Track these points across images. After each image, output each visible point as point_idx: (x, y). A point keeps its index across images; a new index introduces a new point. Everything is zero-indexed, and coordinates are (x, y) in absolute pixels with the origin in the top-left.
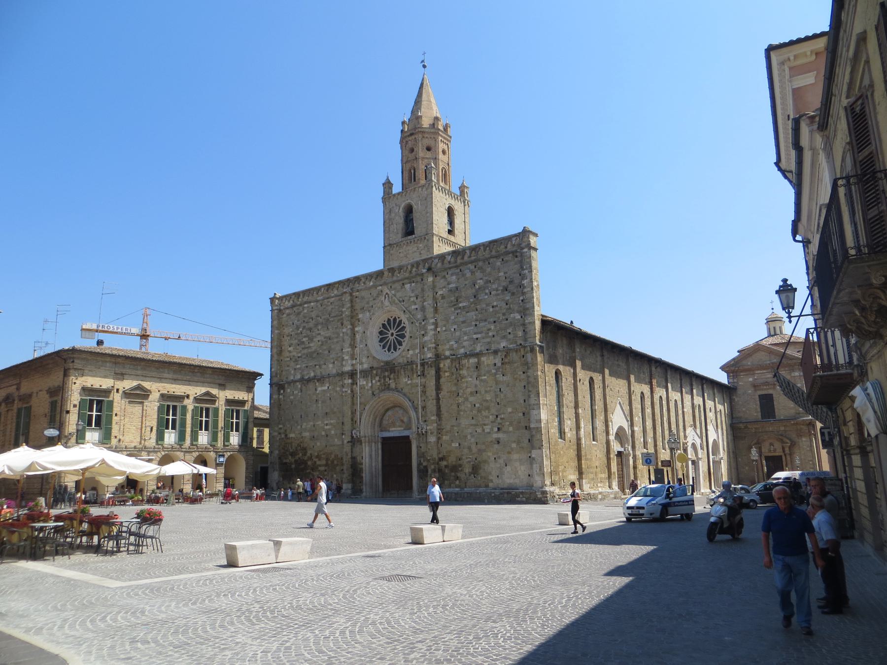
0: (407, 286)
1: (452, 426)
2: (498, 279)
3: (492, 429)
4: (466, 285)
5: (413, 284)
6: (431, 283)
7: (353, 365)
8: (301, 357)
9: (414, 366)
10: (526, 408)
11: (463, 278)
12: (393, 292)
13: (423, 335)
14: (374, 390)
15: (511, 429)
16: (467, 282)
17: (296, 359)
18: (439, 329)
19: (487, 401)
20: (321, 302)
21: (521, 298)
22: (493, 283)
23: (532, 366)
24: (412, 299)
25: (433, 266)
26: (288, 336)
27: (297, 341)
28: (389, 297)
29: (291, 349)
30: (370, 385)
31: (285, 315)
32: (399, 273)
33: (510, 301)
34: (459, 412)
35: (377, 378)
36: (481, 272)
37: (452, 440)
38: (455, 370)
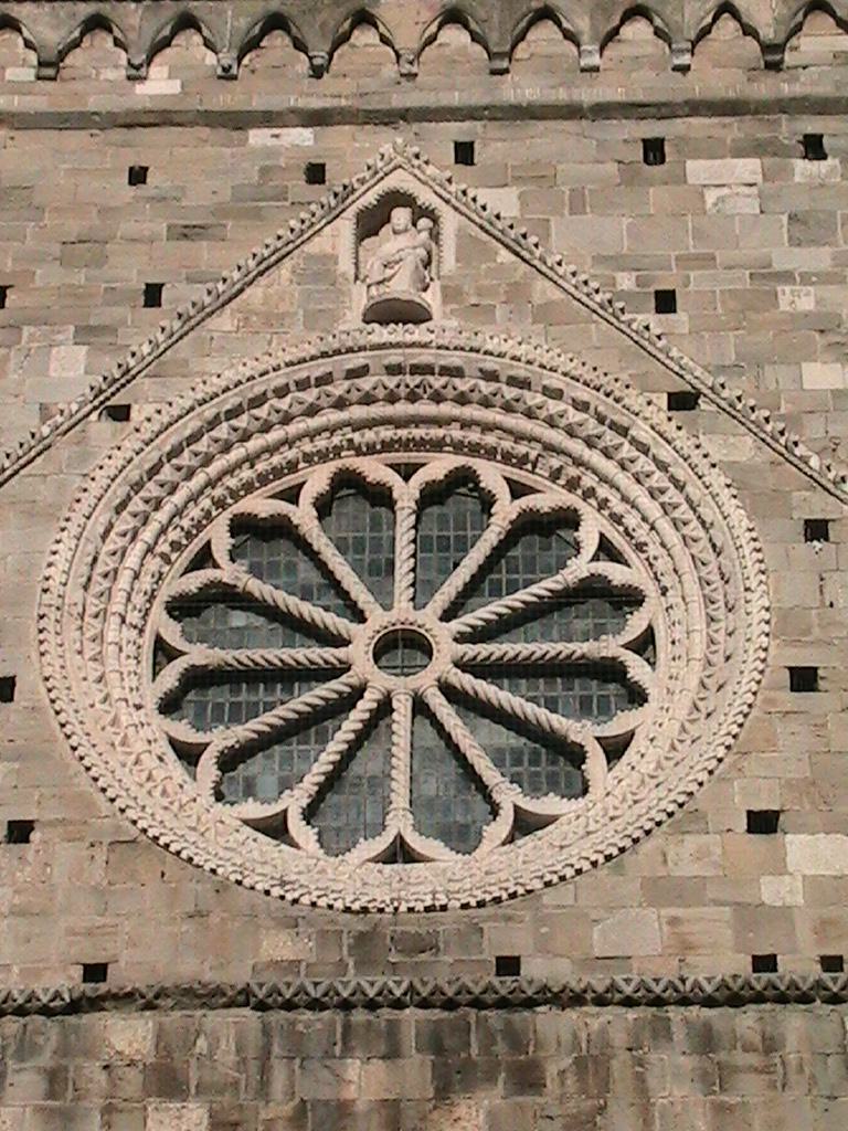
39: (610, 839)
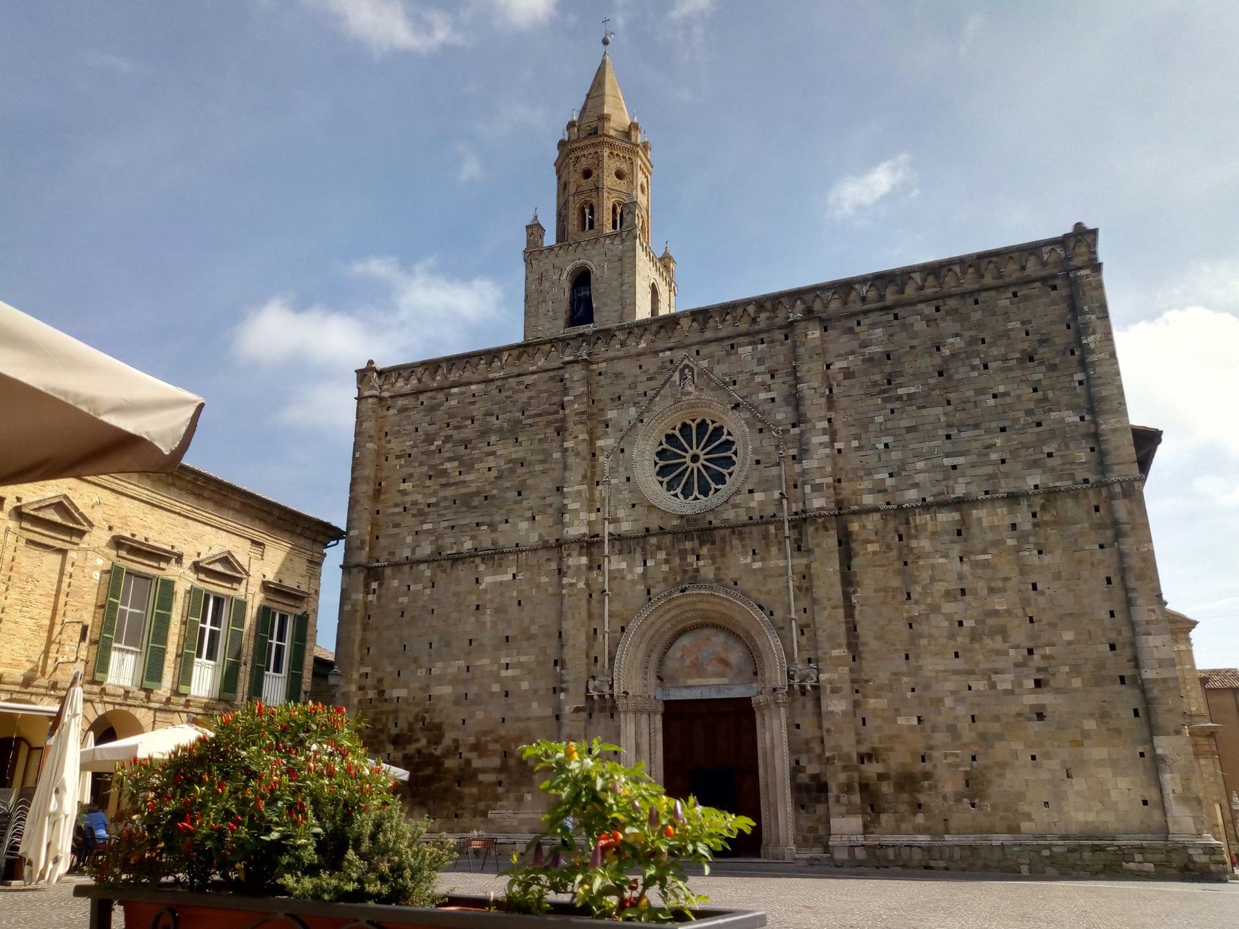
0: (745, 351)
1: (895, 674)
2: (1006, 334)
3: (1018, 683)
4: (912, 347)
5: (760, 346)
7: (590, 524)
8: (436, 504)
9: (772, 529)
10: (1119, 633)
11: (904, 334)
12: (704, 364)
13: (794, 457)
14: (650, 582)
15: (1077, 683)
16: (915, 342)
17: (418, 510)
18: (838, 445)
19: (996, 613)
20: (499, 383)
21: (1079, 376)
22: (993, 344)
23: (1133, 529)
24: (758, 379)
26: (398, 457)
27: (425, 469)
29: (407, 486)
30: (640, 570)
31: (393, 411)
33: (1045, 382)
34: (913, 639)
35: (662, 555)
36: (954, 321)
37: (896, 710)
38: (897, 539)
39: (725, 498)
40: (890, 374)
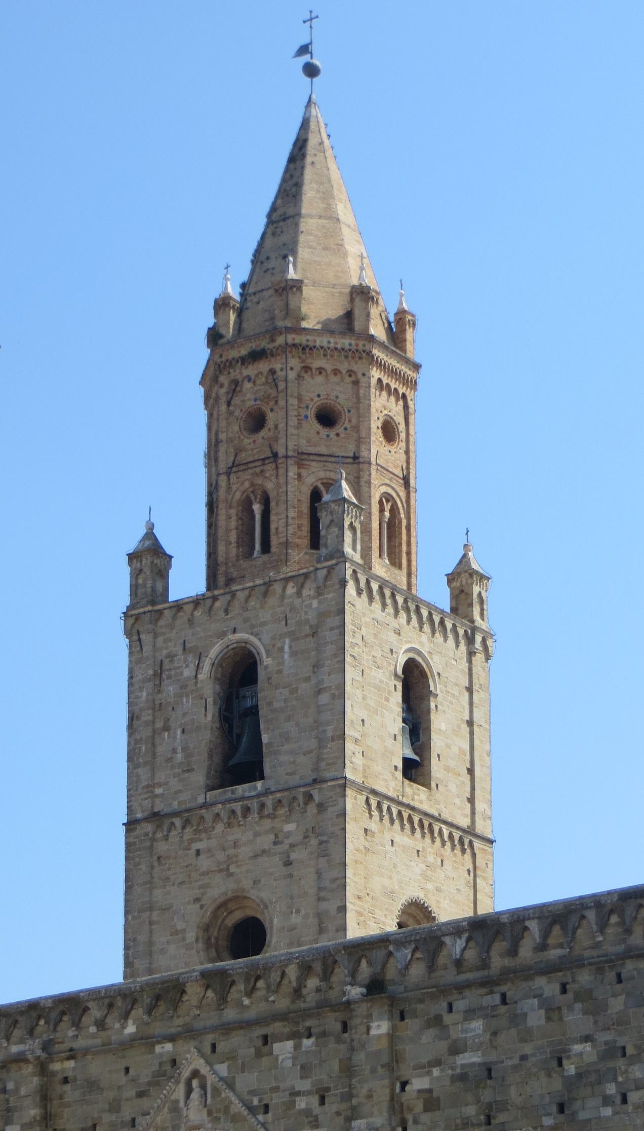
0: (284, 1049)
4: (524, 1058)
5: (307, 1043)
6: (384, 1043)
12: (223, 1069)
24: (301, 1103)
25: (391, 973)
28: (203, 1087)
32: (250, 993)
36: (585, 1013)
40: (489, 1105)
